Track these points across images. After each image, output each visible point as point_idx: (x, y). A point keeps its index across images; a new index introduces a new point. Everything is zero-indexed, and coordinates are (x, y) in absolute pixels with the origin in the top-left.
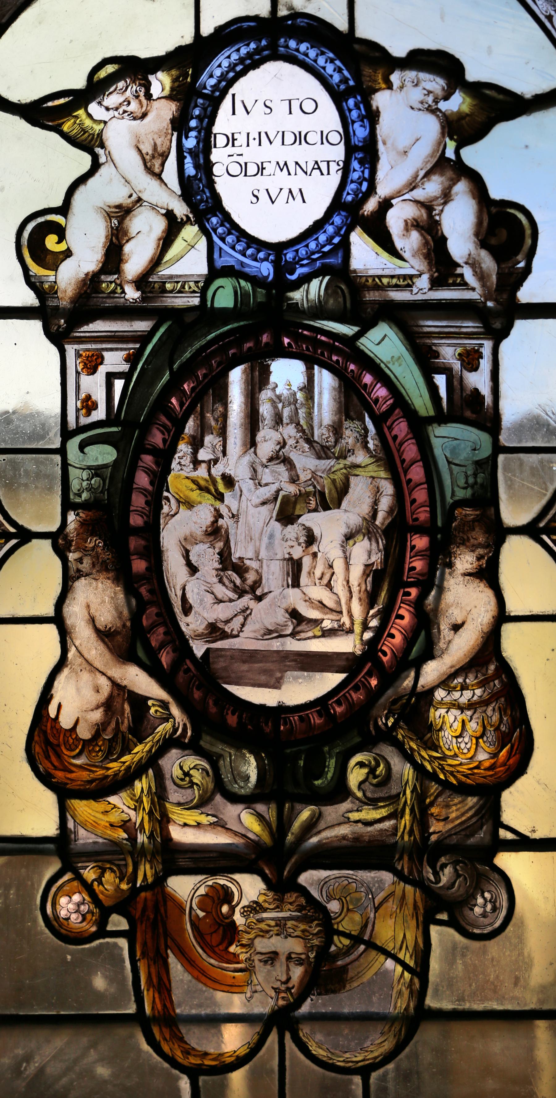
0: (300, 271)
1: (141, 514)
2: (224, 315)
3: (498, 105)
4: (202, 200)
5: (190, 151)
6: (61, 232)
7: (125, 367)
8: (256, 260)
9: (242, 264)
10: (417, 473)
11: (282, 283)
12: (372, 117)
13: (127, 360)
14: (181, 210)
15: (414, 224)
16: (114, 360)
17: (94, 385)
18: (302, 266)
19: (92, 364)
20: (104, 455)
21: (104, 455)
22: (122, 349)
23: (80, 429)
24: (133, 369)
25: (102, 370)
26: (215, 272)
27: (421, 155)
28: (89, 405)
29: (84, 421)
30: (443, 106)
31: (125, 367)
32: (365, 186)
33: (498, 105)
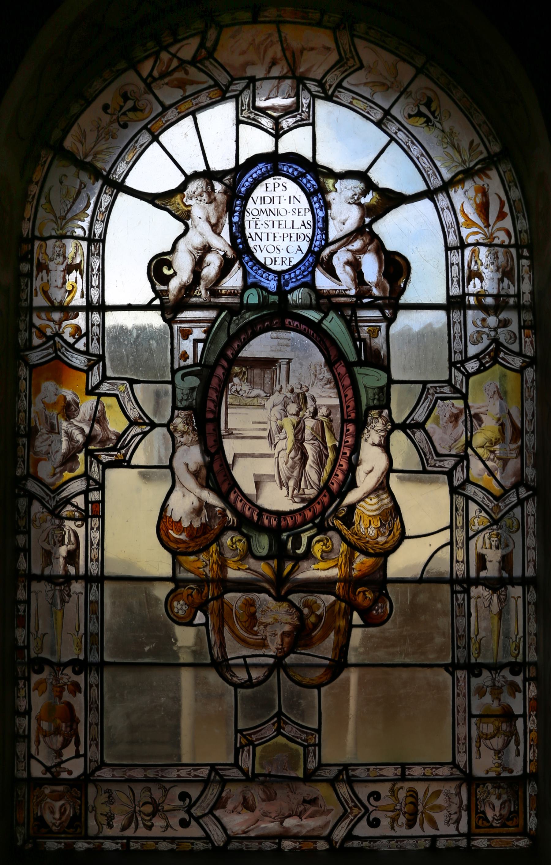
0: (291, 285)
1: (212, 411)
2: (250, 308)
3: (391, 200)
4: (241, 250)
5: (235, 223)
6: (170, 265)
7: (203, 336)
8: (268, 280)
9: (260, 281)
10: (350, 393)
11: (282, 292)
12: (327, 206)
13: (205, 332)
14: (230, 254)
15: (348, 263)
16: (198, 333)
17: (187, 346)
18: (292, 282)
19: (186, 334)
20: (194, 381)
21: (194, 381)
22: (201, 327)
23: (180, 369)
24: (207, 337)
25: (191, 337)
26: (246, 287)
27: (352, 224)
28: (185, 356)
29: (183, 364)
30: (363, 201)
31: (203, 336)
32: (323, 243)
33: (391, 200)
